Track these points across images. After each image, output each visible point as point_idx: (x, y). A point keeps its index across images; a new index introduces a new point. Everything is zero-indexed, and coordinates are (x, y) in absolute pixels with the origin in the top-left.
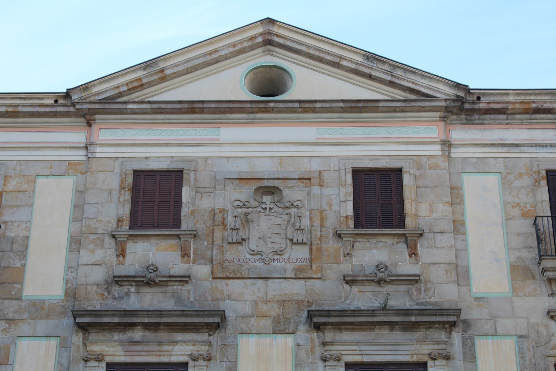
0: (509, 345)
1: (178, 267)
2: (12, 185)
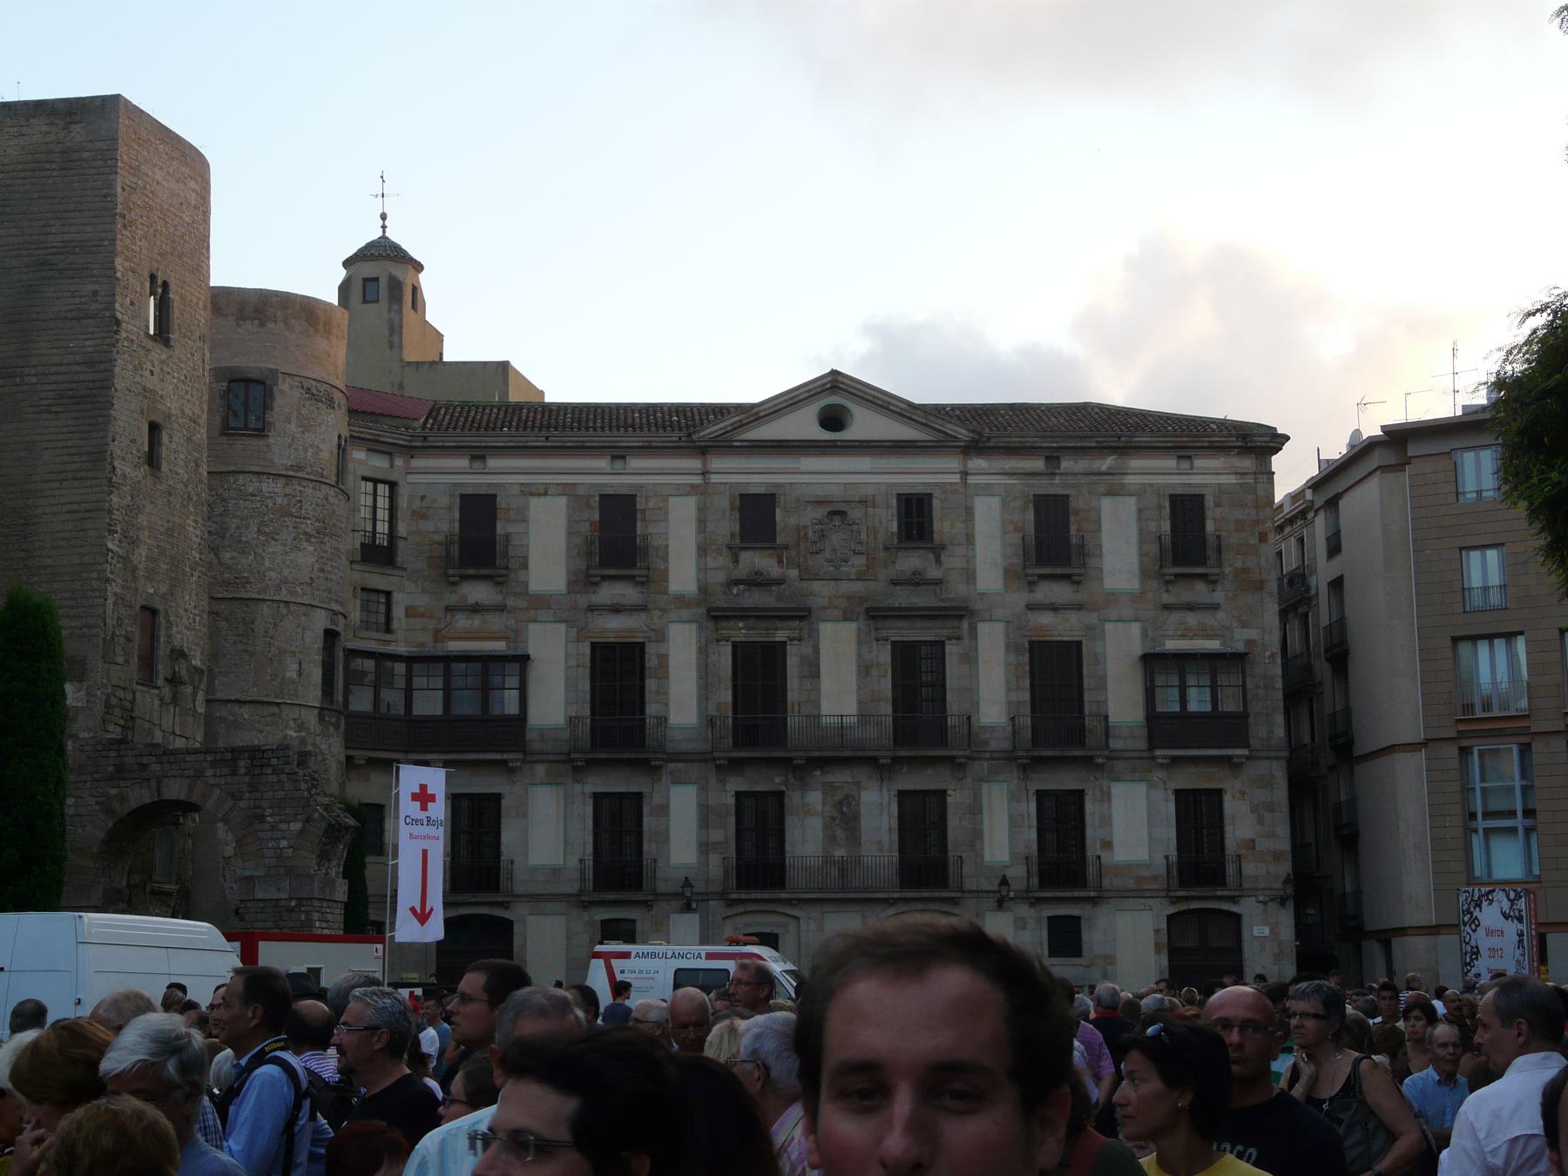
0: (999, 628)
2: (651, 504)
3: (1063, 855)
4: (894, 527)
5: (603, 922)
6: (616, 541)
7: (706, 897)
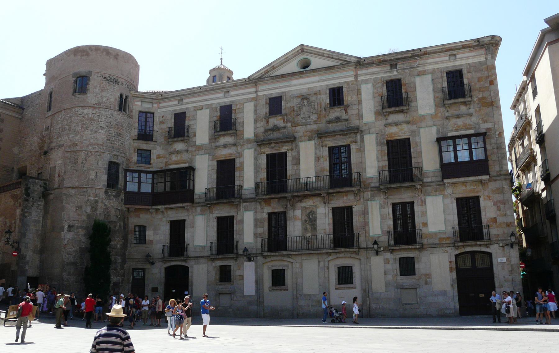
0: (373, 136)
1: (282, 124)
2: (238, 107)
3: (405, 230)
4: (328, 101)
5: (221, 267)
6: (226, 121)
7: (256, 255)
